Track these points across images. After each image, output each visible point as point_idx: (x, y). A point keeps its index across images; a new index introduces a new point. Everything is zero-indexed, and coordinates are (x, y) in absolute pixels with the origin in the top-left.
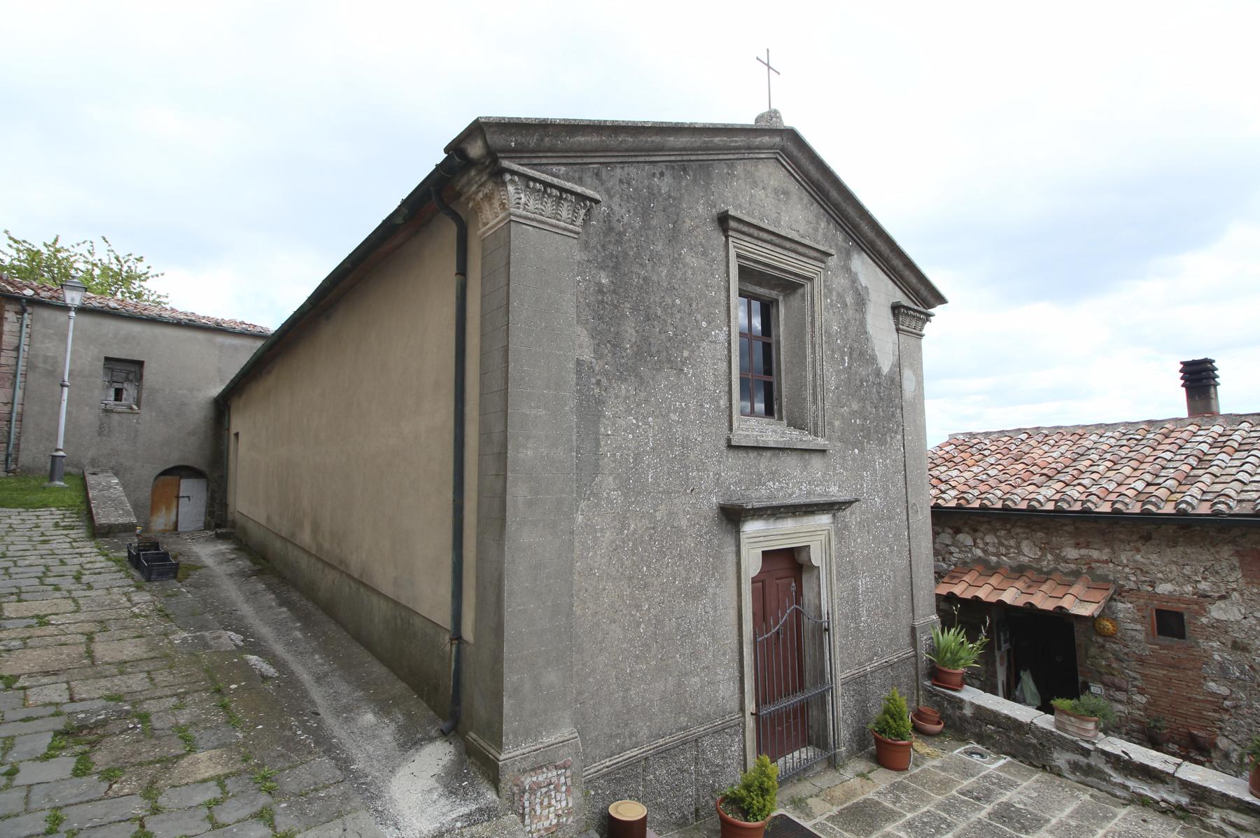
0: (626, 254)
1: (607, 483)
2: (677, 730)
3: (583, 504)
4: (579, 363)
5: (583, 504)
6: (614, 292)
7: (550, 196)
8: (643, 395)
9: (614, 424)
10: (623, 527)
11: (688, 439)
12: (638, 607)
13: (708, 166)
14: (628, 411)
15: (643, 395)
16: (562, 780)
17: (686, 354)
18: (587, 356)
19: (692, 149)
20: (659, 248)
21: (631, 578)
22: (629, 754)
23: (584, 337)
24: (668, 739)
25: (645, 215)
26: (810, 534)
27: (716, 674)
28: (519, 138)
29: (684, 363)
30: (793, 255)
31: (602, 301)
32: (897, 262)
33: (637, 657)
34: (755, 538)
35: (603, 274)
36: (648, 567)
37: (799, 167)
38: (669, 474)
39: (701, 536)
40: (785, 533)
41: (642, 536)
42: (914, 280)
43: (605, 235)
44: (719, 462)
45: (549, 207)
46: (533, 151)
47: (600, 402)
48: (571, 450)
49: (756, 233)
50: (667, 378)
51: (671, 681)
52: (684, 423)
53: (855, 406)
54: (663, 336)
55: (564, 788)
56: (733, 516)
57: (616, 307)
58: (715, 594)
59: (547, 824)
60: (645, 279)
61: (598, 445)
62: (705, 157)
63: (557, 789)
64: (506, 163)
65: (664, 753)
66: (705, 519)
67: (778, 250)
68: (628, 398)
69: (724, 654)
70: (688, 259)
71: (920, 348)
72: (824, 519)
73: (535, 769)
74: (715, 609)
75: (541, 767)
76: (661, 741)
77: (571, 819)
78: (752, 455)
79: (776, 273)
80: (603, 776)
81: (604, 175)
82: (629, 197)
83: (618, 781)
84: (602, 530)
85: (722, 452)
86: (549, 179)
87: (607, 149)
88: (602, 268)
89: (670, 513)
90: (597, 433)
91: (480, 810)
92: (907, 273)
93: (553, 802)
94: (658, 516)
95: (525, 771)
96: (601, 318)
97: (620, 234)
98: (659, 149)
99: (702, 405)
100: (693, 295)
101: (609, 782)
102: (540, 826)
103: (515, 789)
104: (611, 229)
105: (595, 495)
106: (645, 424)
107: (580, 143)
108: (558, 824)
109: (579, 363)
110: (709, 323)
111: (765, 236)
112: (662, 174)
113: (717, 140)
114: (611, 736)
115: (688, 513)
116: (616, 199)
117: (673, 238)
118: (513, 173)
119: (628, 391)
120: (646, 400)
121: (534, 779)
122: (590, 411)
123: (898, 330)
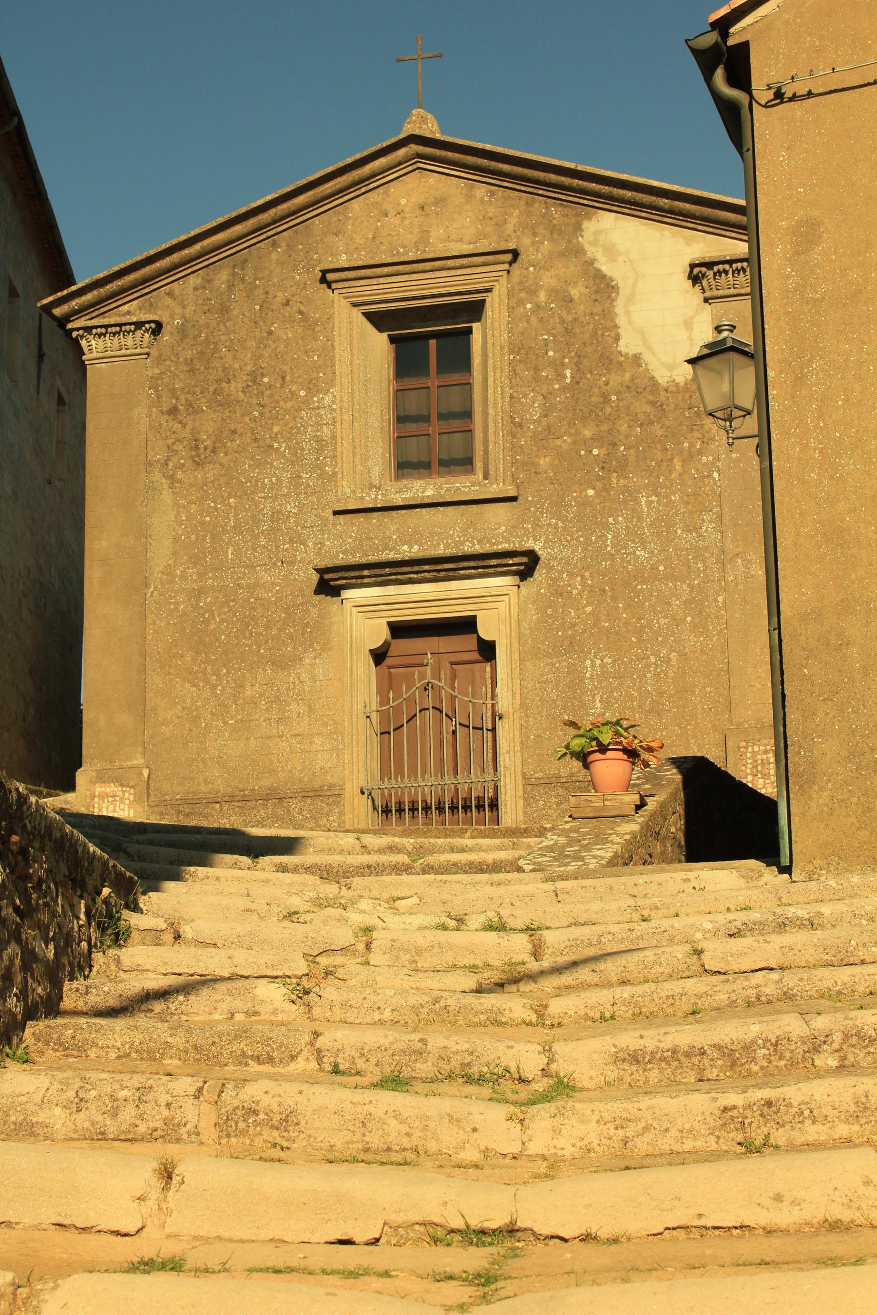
11: (279, 512)
16: (127, 795)
17: (276, 429)
26: (496, 604)
29: (274, 439)
50: (253, 458)
54: (247, 419)
55: (127, 802)
63: (122, 801)
64: (70, 326)
67: (414, 277)
70: (281, 333)
74: (313, 679)
93: (117, 809)
110: (309, 390)
121: (103, 789)
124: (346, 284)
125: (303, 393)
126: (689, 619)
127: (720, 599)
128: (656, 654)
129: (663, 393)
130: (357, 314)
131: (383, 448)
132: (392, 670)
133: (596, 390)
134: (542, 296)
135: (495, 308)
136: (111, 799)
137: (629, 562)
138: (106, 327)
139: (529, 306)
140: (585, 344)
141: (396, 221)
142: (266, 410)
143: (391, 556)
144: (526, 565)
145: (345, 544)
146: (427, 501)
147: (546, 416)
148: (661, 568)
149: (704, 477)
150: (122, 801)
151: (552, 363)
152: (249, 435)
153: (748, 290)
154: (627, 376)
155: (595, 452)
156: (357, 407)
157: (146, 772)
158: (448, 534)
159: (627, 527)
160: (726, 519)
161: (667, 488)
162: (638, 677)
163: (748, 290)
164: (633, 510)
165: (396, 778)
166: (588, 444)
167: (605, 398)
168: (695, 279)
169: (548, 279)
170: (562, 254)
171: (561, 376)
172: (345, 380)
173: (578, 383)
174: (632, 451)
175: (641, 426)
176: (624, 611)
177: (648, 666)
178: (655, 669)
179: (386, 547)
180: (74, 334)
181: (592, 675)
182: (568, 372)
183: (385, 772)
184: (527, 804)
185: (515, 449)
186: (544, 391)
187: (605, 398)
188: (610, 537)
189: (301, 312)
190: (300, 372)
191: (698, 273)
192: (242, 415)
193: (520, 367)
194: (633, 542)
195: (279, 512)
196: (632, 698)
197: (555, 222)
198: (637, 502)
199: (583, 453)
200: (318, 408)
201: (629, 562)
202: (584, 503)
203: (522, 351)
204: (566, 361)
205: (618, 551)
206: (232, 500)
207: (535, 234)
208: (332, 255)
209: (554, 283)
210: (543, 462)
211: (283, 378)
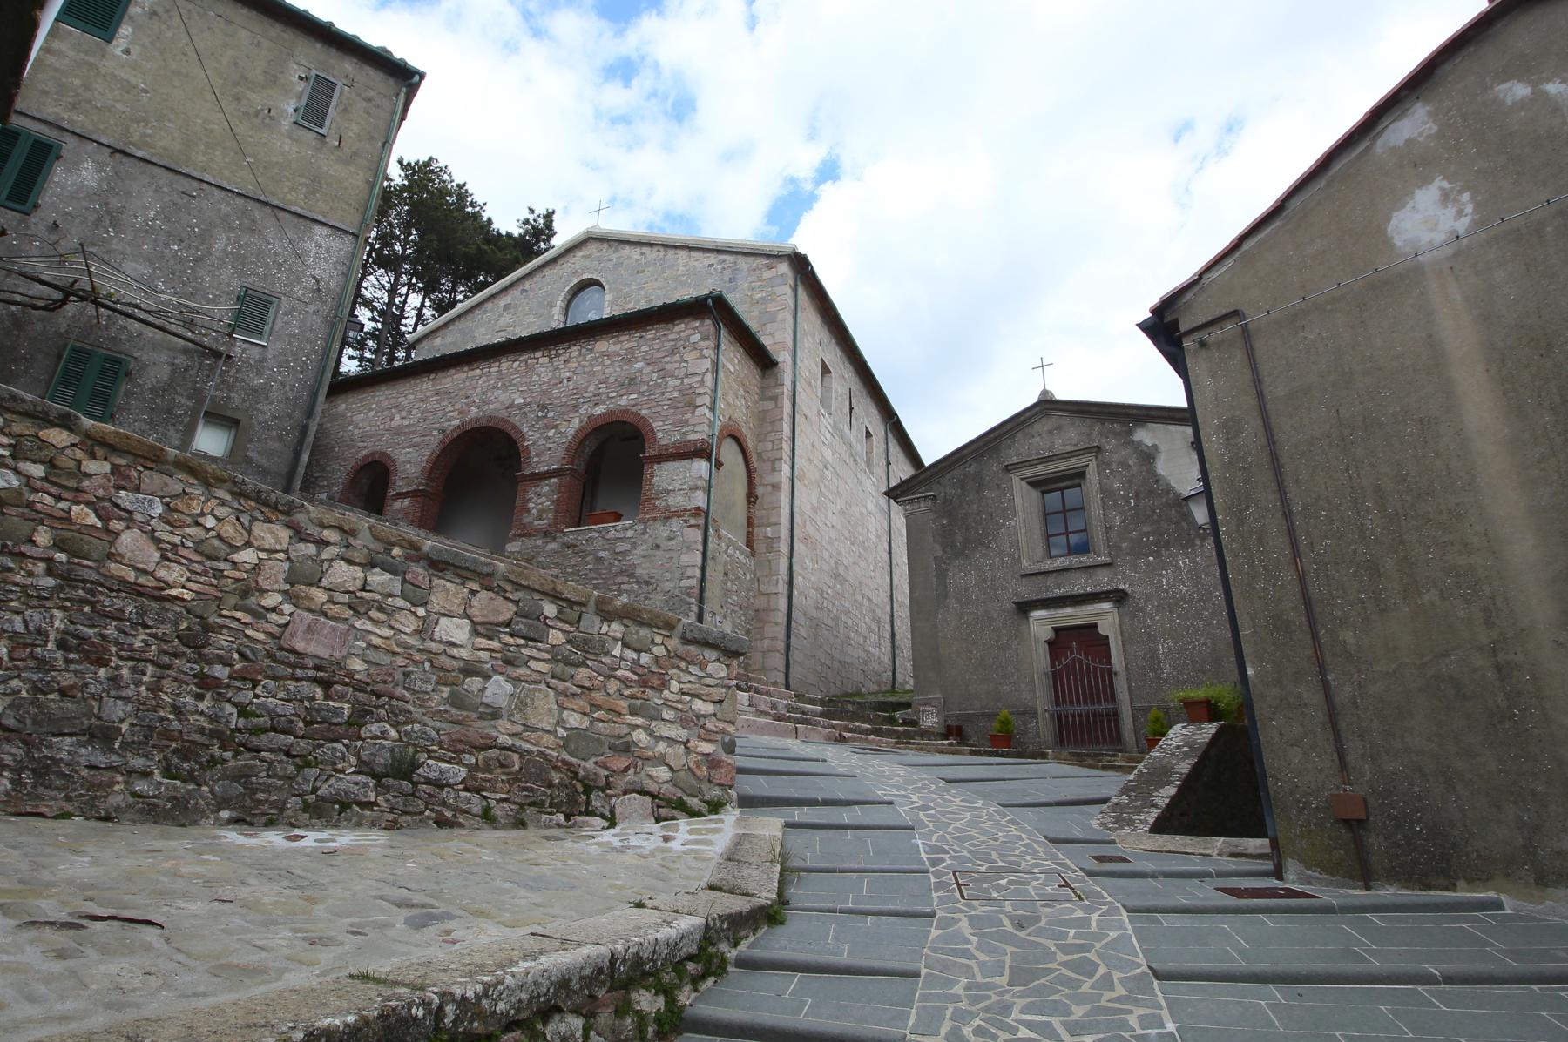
4: (936, 558)
23: (938, 547)
26: (1105, 617)
34: (1041, 620)
40: (1069, 616)
53: (1146, 529)
56: (1024, 608)
72: (1106, 606)
109: (936, 558)
122: (942, 575)
130: (1024, 484)
144: (1119, 598)
145: (1027, 591)
158: (1081, 584)
166: (1147, 535)
183: (1057, 703)
185: (1109, 540)
202: (1149, 564)
203: (1106, 492)
210: (1124, 545)
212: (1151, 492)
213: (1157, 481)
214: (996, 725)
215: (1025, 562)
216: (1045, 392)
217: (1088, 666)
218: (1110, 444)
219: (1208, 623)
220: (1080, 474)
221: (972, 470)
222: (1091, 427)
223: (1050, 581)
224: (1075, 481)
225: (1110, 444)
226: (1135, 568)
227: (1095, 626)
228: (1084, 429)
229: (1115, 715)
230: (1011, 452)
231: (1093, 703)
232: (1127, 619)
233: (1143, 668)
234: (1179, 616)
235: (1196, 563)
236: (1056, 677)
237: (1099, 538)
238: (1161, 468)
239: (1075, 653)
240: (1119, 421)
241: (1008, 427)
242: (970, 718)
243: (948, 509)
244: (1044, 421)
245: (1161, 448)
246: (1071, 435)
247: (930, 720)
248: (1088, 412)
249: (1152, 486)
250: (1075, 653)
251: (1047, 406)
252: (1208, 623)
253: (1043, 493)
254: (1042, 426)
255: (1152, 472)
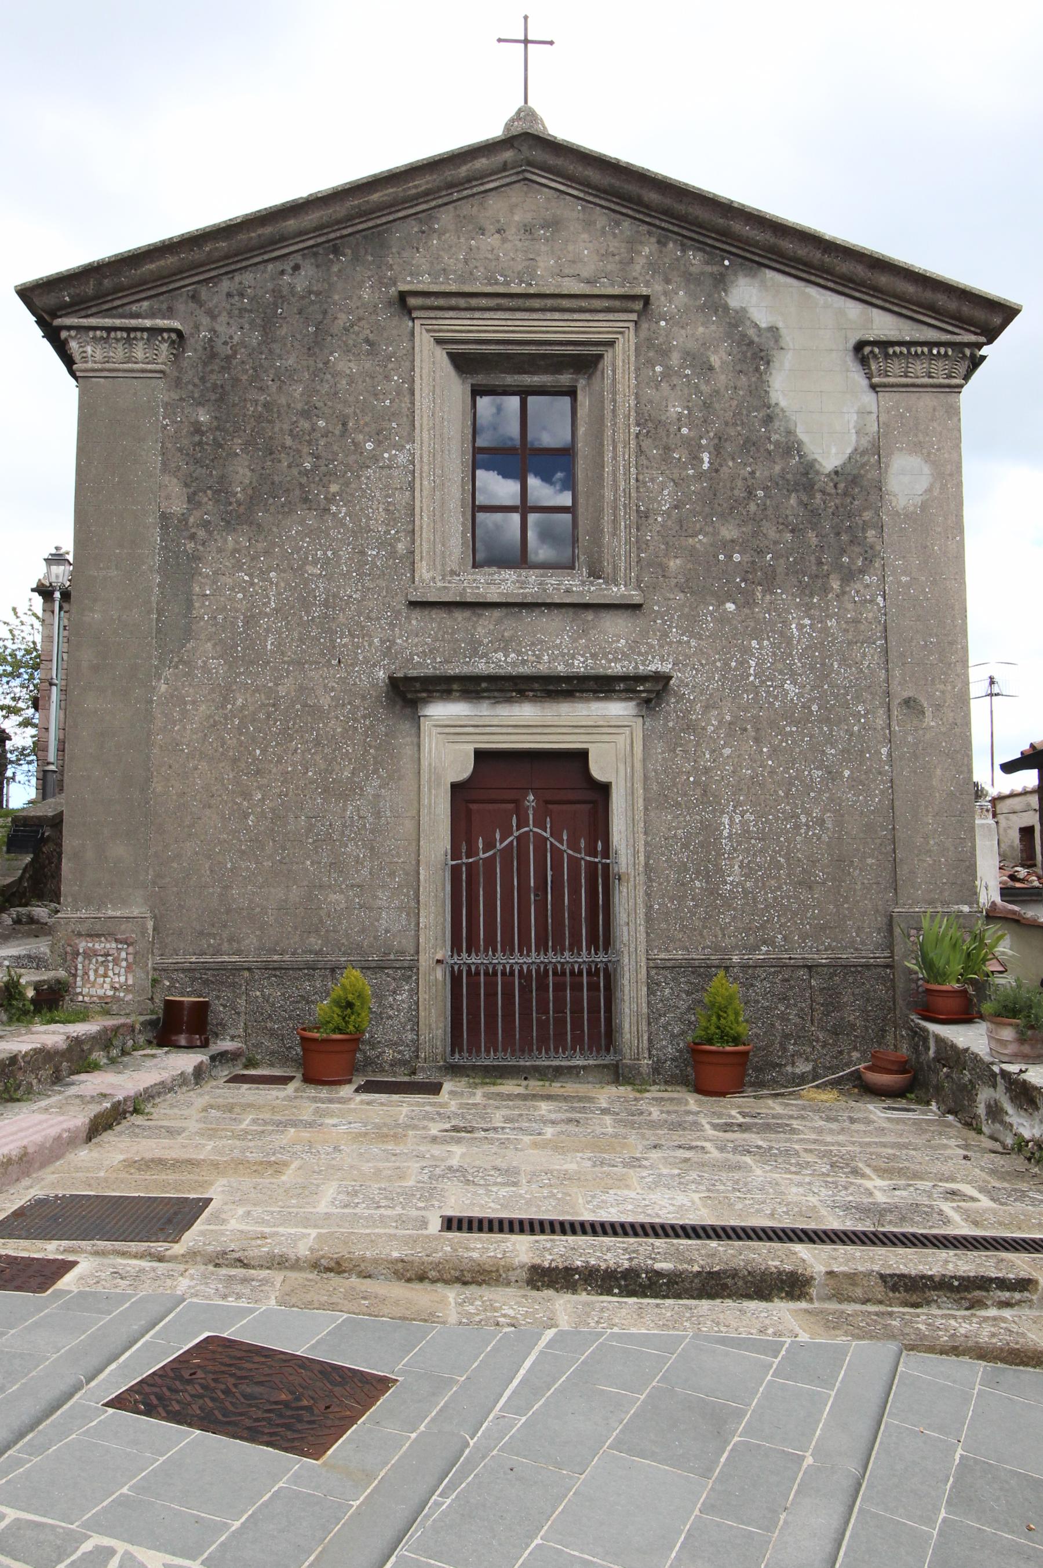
0: (236, 381)
1: (206, 653)
2: (304, 952)
3: (168, 673)
4: (164, 516)
5: (168, 673)
6: (217, 428)
7: (117, 340)
8: (261, 546)
9: (215, 582)
10: (226, 699)
11: (335, 596)
12: (247, 795)
13: (380, 234)
14: (239, 566)
15: (261, 546)
16: (123, 955)
17: (334, 488)
18: (178, 507)
19: (338, 222)
20: (290, 362)
21: (235, 760)
22: (226, 958)
23: (175, 487)
24: (287, 958)
25: (268, 325)
26: (609, 736)
27: (375, 897)
28: (72, 291)
29: (331, 499)
30: (557, 315)
31: (200, 443)
32: (845, 267)
33: (243, 852)
34: (453, 730)
35: (201, 411)
36: (264, 751)
37: (571, 179)
38: (301, 641)
39: (355, 720)
41: (254, 713)
42: (910, 289)
43: (205, 364)
44: (392, 626)
45: (119, 352)
46: (96, 297)
47: (197, 558)
48: (149, 612)
49: (462, 302)
50: (302, 522)
51: (295, 893)
52: (329, 578)
53: (729, 532)
54: (295, 471)
55: (124, 964)
56: (408, 693)
57: (221, 446)
58: (377, 796)
59: (101, 992)
60: (266, 405)
61: (189, 605)
62: (370, 224)
63: (116, 962)
64: (58, 322)
65: (276, 971)
66: (364, 698)
67: (519, 315)
68: (238, 551)
69: (392, 874)
70: (341, 366)
71: (954, 412)
72: (618, 710)
73: (92, 935)
74: (378, 815)
75: (98, 936)
76: (276, 957)
77: (130, 997)
78: (459, 615)
79: (532, 349)
80: (184, 970)
81: (204, 293)
82: (242, 311)
83: (206, 983)
84: (194, 702)
85: (397, 614)
86: (108, 322)
87: (194, 267)
88: (200, 404)
89: (301, 689)
90: (189, 593)
91: (29, 957)
92: (883, 280)
93: (110, 973)
94: (282, 691)
95: (80, 935)
96: (197, 462)
97: (228, 358)
98: (282, 239)
99: (363, 553)
100: (349, 411)
101: (193, 980)
102: (93, 992)
103: (69, 949)
104: (213, 356)
105: (185, 663)
106: (264, 580)
107: (151, 271)
108: (113, 997)
109: (164, 516)
111: (484, 302)
112: (296, 268)
113: (375, 197)
114: (201, 933)
115: (333, 689)
116: (223, 318)
117: (316, 344)
118: (69, 328)
119: (237, 542)
120: (266, 553)
121: (90, 945)
122: (180, 569)
123: (873, 387)
124: (432, 314)
125: (369, 446)
126: (847, 773)
127: (884, 751)
128: (808, 814)
129: (818, 496)
130: (441, 355)
131: (463, 524)
132: (474, 807)
133: (740, 483)
134: (675, 359)
135: (621, 364)
136: (101, 959)
137: (776, 698)
138: (109, 329)
139: (658, 369)
140: (727, 424)
141: (494, 240)
142: (322, 462)
143: (482, 667)
144: (649, 691)
145: (423, 647)
146: (529, 600)
147: (676, 507)
148: (815, 708)
149: (866, 600)
150: (116, 962)
151: (687, 441)
152: (297, 492)
153: (514, 402)
154: (777, 468)
155: (737, 557)
156: (439, 472)
157: (150, 924)
159: (774, 654)
160: (893, 655)
161: (821, 610)
162: (787, 840)
163: (514, 402)
164: (782, 634)
165: (486, 951)
166: (728, 546)
167: (750, 493)
168: (864, 361)
169: (680, 339)
170: (701, 308)
171: (697, 459)
172: (425, 435)
173: (717, 471)
174: (782, 561)
175: (793, 531)
176: (769, 758)
177: (797, 827)
178: (806, 833)
179: (475, 653)
180: (64, 334)
181: (730, 835)
182: (706, 457)
184: (651, 992)
185: (640, 545)
186: (676, 476)
187: (750, 493)
188: (753, 663)
189: (367, 341)
190: (367, 419)
191: (863, 352)
192: (289, 466)
193: (646, 443)
194: (781, 672)
195: (335, 596)
196: (780, 867)
197: (693, 269)
198: (786, 623)
199: (721, 557)
200: (390, 467)
201: (776, 698)
202: (723, 619)
203: (650, 424)
204: (704, 442)
205: (762, 682)
206: (272, 574)
207: (668, 281)
208: (411, 274)
209: (692, 345)
210: (674, 564)
211: (344, 424)
212: (750, 445)
213: (769, 420)
214: (323, 1007)
215: (424, 571)
216: (526, 114)
217: (574, 863)
218: (673, 300)
219: (833, 775)
220: (585, 362)
221: (301, 283)
222: (632, 244)
223: (485, 626)
224: (565, 379)
225: (673, 300)
226: (691, 623)
227: (582, 756)
228: (614, 245)
229: (604, 983)
230: (420, 259)
231: (559, 947)
232: (659, 747)
233: (683, 868)
234: (775, 750)
235: (825, 629)
236: (464, 885)
237: (617, 546)
238: (783, 387)
239: (532, 825)
240: (701, 246)
241: (423, 183)
242: (225, 975)
243: (217, 381)
244: (516, 194)
245: (789, 338)
246: (582, 252)
247: (109, 980)
248: (637, 202)
249: (754, 432)
250: (532, 825)
251: (529, 155)
252: (833, 775)
253: (477, 392)
254: (514, 207)
255: (759, 393)
